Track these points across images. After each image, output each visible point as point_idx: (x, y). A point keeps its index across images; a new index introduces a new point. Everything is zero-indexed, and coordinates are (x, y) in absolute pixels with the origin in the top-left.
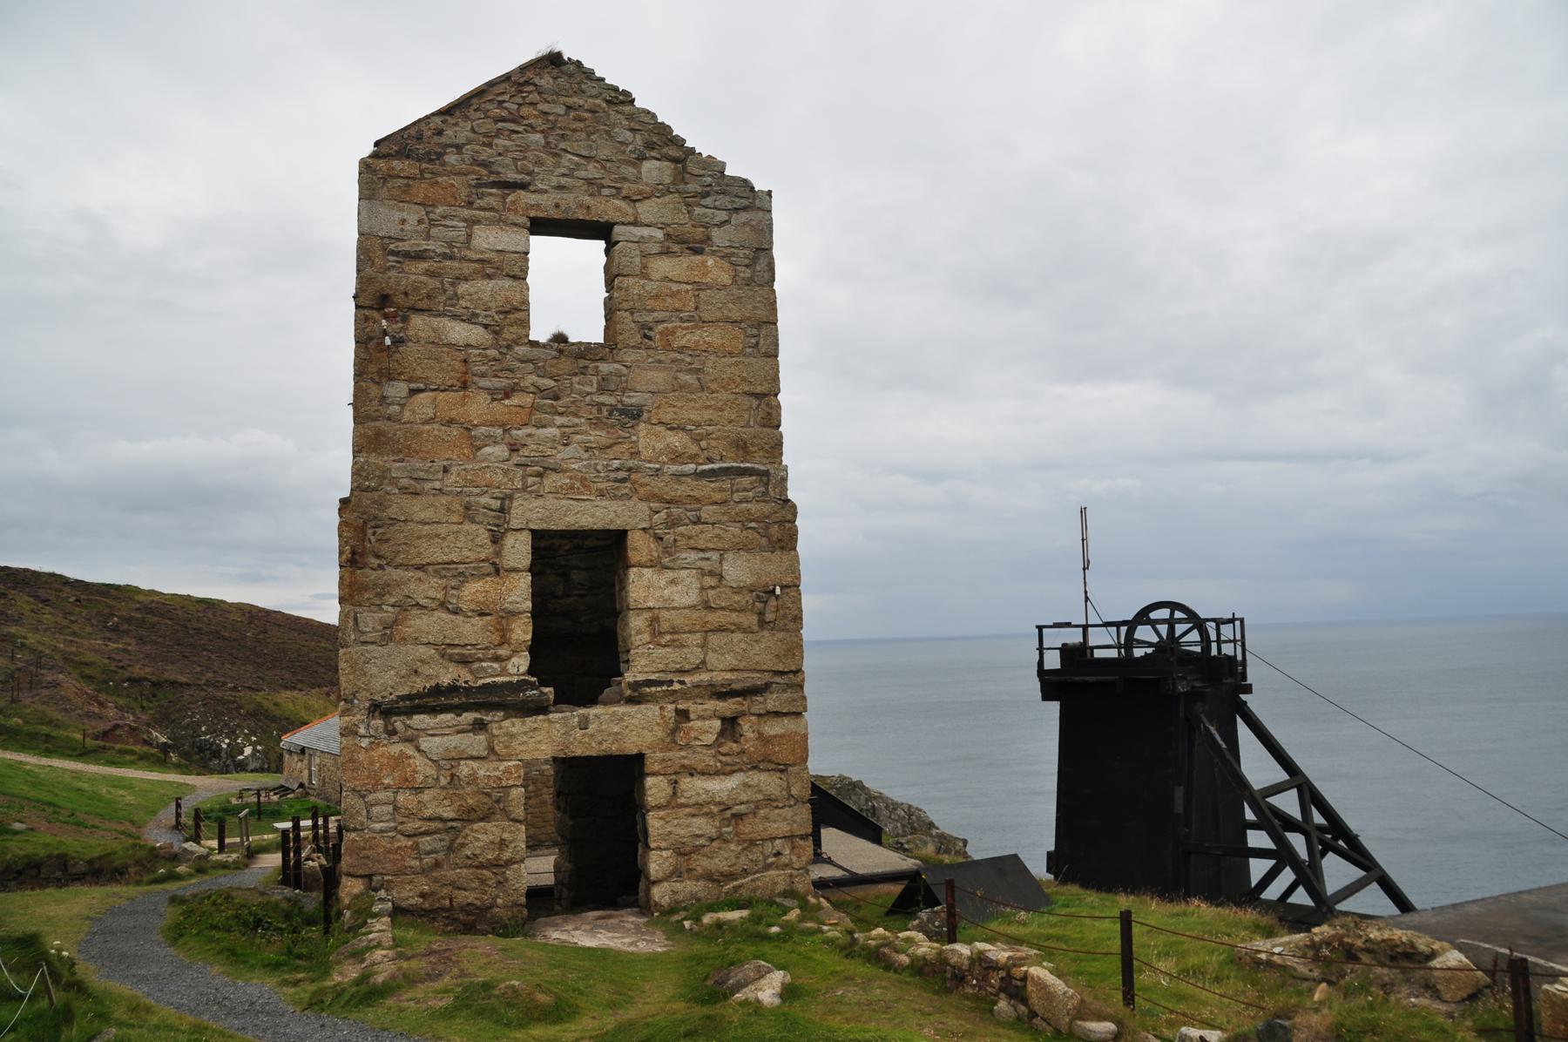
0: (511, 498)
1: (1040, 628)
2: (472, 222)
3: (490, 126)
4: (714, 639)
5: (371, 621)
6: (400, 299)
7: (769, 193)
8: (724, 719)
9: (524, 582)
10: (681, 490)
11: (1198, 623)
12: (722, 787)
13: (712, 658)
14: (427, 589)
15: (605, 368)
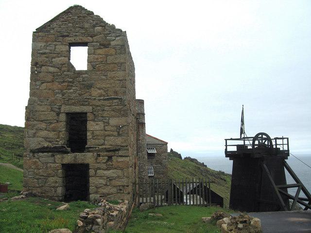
0: (61, 106)
1: (226, 140)
2: (55, 45)
3: (61, 23)
4: (107, 138)
5: (31, 132)
6: (40, 63)
7: (125, 32)
8: (109, 157)
10: (100, 103)
11: (268, 139)
12: (107, 173)
14: (43, 125)
15: (84, 76)
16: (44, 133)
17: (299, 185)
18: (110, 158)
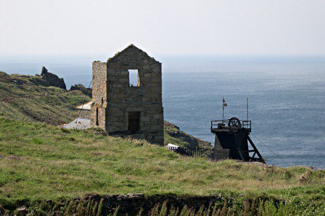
9: (127, 118)
11: (239, 121)
13: (152, 128)
14: (116, 119)
16: (117, 124)
17: (256, 151)
18: (153, 137)
